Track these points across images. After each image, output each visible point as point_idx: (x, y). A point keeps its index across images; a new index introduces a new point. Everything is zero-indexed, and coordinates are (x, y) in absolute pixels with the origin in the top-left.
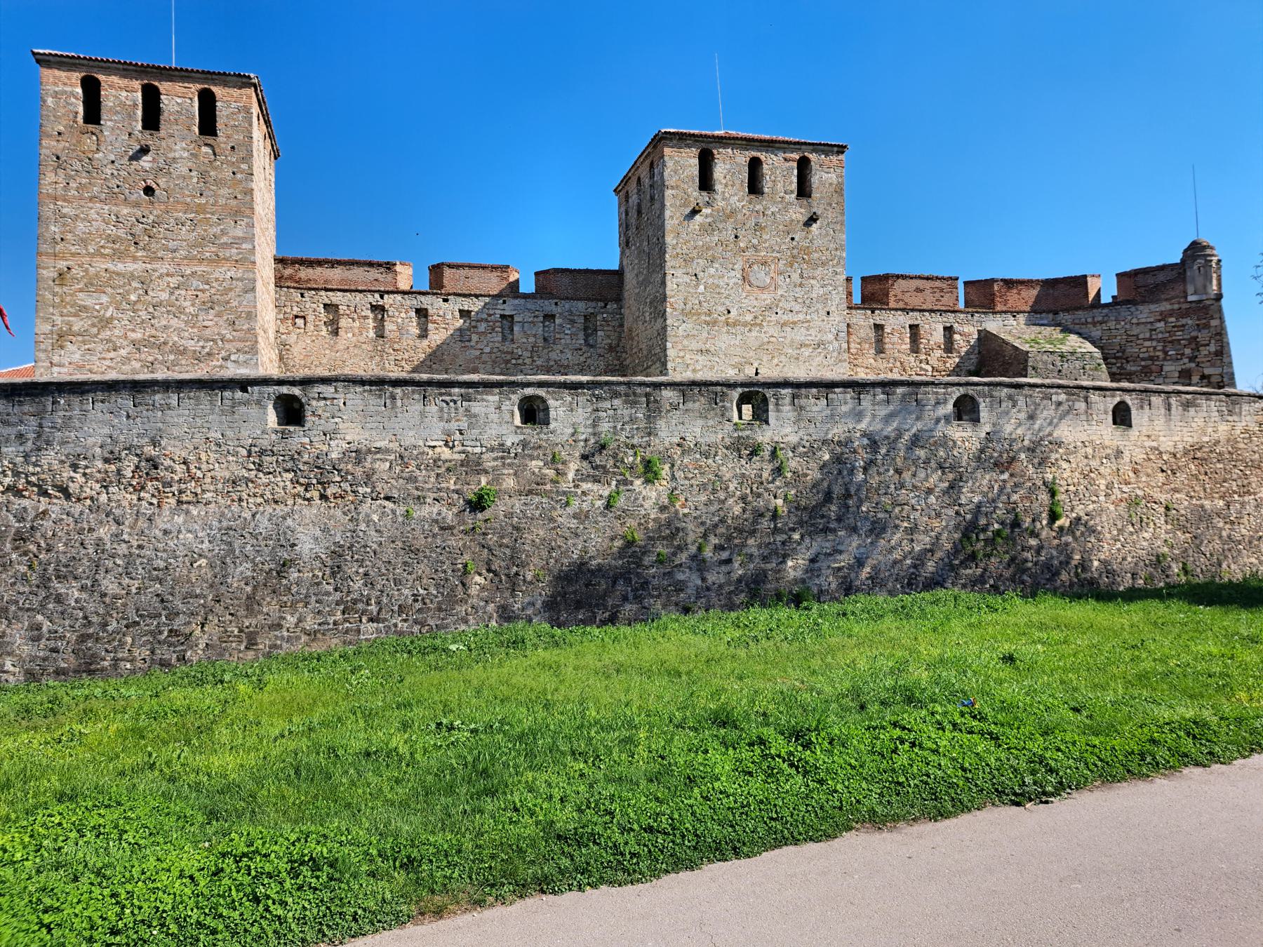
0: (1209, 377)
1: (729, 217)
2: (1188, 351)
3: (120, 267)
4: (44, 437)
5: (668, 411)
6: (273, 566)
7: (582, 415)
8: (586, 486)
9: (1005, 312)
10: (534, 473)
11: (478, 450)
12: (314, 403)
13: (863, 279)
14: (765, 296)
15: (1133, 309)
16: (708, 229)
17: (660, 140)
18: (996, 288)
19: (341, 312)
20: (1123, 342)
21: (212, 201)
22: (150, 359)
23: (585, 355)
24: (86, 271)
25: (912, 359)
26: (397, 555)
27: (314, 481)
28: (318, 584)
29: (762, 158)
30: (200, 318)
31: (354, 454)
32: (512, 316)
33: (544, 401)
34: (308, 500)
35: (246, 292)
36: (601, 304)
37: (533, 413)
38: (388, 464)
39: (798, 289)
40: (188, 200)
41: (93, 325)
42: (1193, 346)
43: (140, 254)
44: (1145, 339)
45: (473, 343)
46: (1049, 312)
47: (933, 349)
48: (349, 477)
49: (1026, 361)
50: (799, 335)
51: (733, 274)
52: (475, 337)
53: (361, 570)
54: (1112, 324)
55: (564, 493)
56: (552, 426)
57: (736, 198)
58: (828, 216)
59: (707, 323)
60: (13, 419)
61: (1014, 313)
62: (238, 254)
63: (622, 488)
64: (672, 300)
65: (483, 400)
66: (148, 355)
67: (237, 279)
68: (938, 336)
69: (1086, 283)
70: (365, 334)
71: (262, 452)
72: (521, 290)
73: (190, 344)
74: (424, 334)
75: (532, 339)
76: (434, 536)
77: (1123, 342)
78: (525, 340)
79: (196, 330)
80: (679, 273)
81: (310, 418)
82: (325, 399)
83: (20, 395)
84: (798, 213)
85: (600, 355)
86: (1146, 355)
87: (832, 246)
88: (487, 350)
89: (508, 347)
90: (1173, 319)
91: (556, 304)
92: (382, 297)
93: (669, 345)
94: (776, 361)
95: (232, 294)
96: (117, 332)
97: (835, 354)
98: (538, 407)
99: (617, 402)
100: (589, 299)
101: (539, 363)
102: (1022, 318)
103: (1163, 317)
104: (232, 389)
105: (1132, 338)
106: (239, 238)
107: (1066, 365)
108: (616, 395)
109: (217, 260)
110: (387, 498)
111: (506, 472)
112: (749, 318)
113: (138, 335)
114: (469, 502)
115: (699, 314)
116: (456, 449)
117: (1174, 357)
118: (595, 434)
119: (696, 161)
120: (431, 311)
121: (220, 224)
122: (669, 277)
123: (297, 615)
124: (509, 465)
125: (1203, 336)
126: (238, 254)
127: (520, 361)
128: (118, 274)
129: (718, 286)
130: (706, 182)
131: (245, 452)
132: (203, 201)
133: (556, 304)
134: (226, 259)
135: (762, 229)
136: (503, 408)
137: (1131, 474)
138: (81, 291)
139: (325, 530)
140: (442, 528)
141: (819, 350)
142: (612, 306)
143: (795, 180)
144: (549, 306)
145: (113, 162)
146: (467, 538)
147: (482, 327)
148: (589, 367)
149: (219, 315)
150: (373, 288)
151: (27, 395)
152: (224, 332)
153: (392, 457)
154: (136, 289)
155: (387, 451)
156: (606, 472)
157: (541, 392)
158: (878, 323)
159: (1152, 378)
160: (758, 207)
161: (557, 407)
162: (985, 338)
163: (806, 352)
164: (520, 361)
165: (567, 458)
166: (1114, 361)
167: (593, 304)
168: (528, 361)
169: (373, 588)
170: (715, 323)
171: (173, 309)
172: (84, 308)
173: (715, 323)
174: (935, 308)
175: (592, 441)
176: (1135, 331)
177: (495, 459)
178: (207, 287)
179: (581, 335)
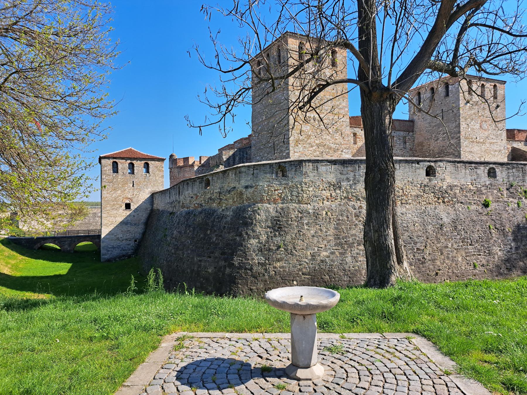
4: (356, 179)
6: (439, 226)
9: (518, 141)
11: (479, 186)
12: (438, 168)
14: (486, 133)
18: (515, 132)
22: (322, 151)
30: (335, 136)
34: (439, 203)
36: (408, 133)
39: (494, 131)
41: (306, 138)
50: (495, 147)
51: (478, 125)
55: (506, 202)
56: (497, 178)
59: (471, 142)
60: (344, 172)
61: (520, 141)
63: (520, 200)
65: (480, 169)
66: (321, 149)
71: (425, 186)
73: (333, 146)
74: (355, 143)
80: (464, 123)
81: (437, 174)
82: (441, 167)
83: (346, 164)
87: (503, 116)
94: (489, 156)
95: (343, 127)
99: (514, 170)
100: (404, 131)
102: (523, 143)
104: (415, 163)
106: (344, 106)
108: (513, 168)
110: (461, 203)
112: (482, 140)
113: (317, 142)
114: (484, 204)
115: (469, 139)
120: (358, 134)
122: (461, 125)
123: (451, 243)
124: (489, 192)
129: (474, 129)
131: (419, 186)
136: (485, 171)
139: (448, 213)
140: (479, 213)
142: (411, 134)
146: (487, 217)
151: (349, 164)
153: (459, 188)
156: (515, 195)
157: (494, 166)
163: (497, 153)
165: (503, 189)
167: (405, 133)
169: (467, 234)
175: (508, 184)
179: (402, 144)
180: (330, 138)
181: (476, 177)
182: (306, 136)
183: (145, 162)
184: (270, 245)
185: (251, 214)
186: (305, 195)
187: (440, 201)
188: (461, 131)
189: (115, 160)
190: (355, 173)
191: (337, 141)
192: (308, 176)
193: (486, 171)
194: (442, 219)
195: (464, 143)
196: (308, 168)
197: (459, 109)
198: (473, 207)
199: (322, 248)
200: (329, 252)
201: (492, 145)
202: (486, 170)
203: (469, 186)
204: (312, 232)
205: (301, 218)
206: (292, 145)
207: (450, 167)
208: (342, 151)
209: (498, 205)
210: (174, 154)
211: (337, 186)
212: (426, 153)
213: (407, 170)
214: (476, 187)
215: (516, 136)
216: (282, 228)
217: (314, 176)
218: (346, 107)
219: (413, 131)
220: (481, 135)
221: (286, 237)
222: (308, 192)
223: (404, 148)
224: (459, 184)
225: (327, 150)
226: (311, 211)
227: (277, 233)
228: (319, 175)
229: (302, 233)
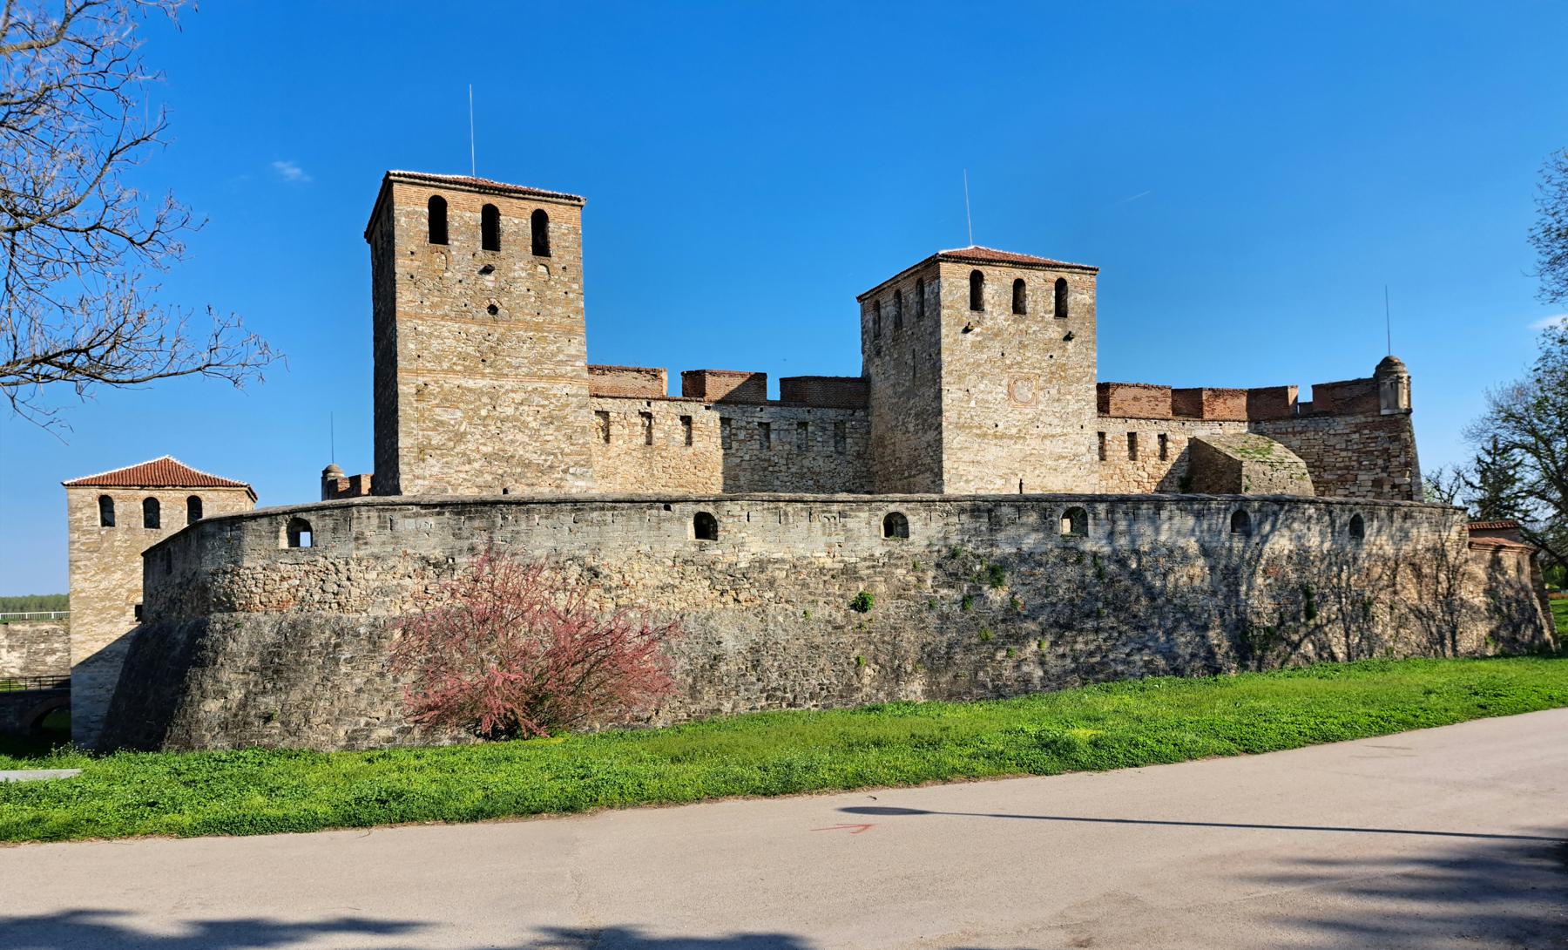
0: (1399, 486)
1: (996, 335)
2: (1380, 462)
3: (470, 383)
5: (1007, 525)
7: (935, 527)
9: (1213, 420)
10: (899, 580)
14: (1027, 411)
15: (1330, 421)
16: (978, 347)
17: (932, 263)
18: (1204, 398)
19: (611, 419)
20: (1321, 452)
21: (548, 319)
22: (500, 472)
23: (835, 462)
24: (441, 387)
25: (1130, 467)
26: (802, 652)
27: (728, 588)
28: (744, 675)
29: (1025, 279)
30: (542, 433)
31: (757, 564)
33: (903, 517)
35: (581, 408)
36: (849, 412)
37: (895, 526)
39: (1056, 404)
40: (528, 318)
42: (1385, 457)
43: (487, 371)
44: (1341, 450)
45: (733, 451)
47: (1148, 457)
48: (757, 584)
49: (1240, 470)
50: (1057, 447)
51: (1000, 389)
52: (735, 445)
53: (776, 664)
54: (1311, 435)
56: (912, 537)
57: (1003, 317)
58: (1082, 335)
59: (978, 435)
62: (573, 371)
64: (947, 414)
65: (856, 516)
67: (573, 396)
68: (1154, 444)
69: (1287, 394)
70: (635, 441)
72: (769, 398)
74: (689, 442)
75: (787, 447)
76: (830, 634)
77: (1321, 452)
78: (781, 448)
79: (538, 444)
80: (953, 388)
81: (721, 534)
82: (733, 516)
84: (1055, 332)
85: (849, 463)
86: (1342, 465)
88: (747, 457)
89: (765, 454)
90: (1367, 431)
91: (809, 412)
92: (649, 404)
93: (945, 457)
94: (1037, 472)
95: (568, 410)
96: (470, 446)
97: (1088, 466)
98: (896, 522)
100: (839, 407)
101: (793, 470)
103: (1358, 429)
105: (1328, 449)
106: (573, 356)
107: (1275, 475)
109: (555, 377)
110: (787, 602)
111: (878, 579)
112: (1014, 431)
113: (487, 449)
115: (971, 427)
116: (835, 559)
117: (1368, 467)
118: (946, 546)
120: (695, 419)
121: (555, 343)
124: (880, 573)
125: (1394, 448)
126: (573, 371)
127: (776, 469)
128: (470, 390)
130: (976, 303)
132: (540, 319)
134: (563, 376)
135: (1025, 346)
138: (438, 406)
139: (743, 629)
141: (1075, 462)
142: (859, 414)
143: (1054, 301)
144: (801, 413)
145: (460, 281)
147: (742, 435)
149: (558, 429)
150: (641, 396)
152: (563, 446)
154: (485, 405)
155: (783, 561)
159: (1347, 486)
160: (1022, 326)
161: (915, 523)
162: (1195, 444)
163: (1063, 463)
164: (776, 469)
165: (925, 567)
167: (842, 412)
168: (783, 468)
170: (985, 435)
171: (519, 424)
172: (442, 423)
173: (985, 435)
174: (1151, 416)
176: (1333, 441)
177: (868, 568)
178: (546, 403)
179: (832, 442)
180: (527, 440)
181: (842, 538)
182: (451, 435)
183: (145, 494)
184: (248, 715)
185: (218, 640)
186: (355, 592)
187: (728, 598)
188: (944, 407)
189: (104, 492)
190: (491, 533)
191: (548, 446)
192: (366, 544)
193: (878, 522)
194: (719, 643)
195: (952, 439)
196: (365, 521)
197: (939, 353)
198: (821, 612)
199: (378, 719)
200: (395, 728)
201: (1047, 442)
202: (876, 518)
203: (822, 560)
204: (357, 680)
205: (337, 645)
206: (406, 460)
207: (760, 515)
208: (565, 471)
209: (897, 607)
210: (335, 466)
211: (442, 567)
212: (890, 464)
213: (636, 523)
214: (842, 561)
215: (1206, 408)
216: (282, 672)
217: (384, 543)
218: (577, 357)
219: (866, 407)
220: (1009, 419)
221: (288, 694)
222: (363, 582)
223: (837, 452)
224: (788, 556)
225: (519, 470)
226: (362, 630)
227: (269, 686)
228: (396, 539)
229: (330, 684)
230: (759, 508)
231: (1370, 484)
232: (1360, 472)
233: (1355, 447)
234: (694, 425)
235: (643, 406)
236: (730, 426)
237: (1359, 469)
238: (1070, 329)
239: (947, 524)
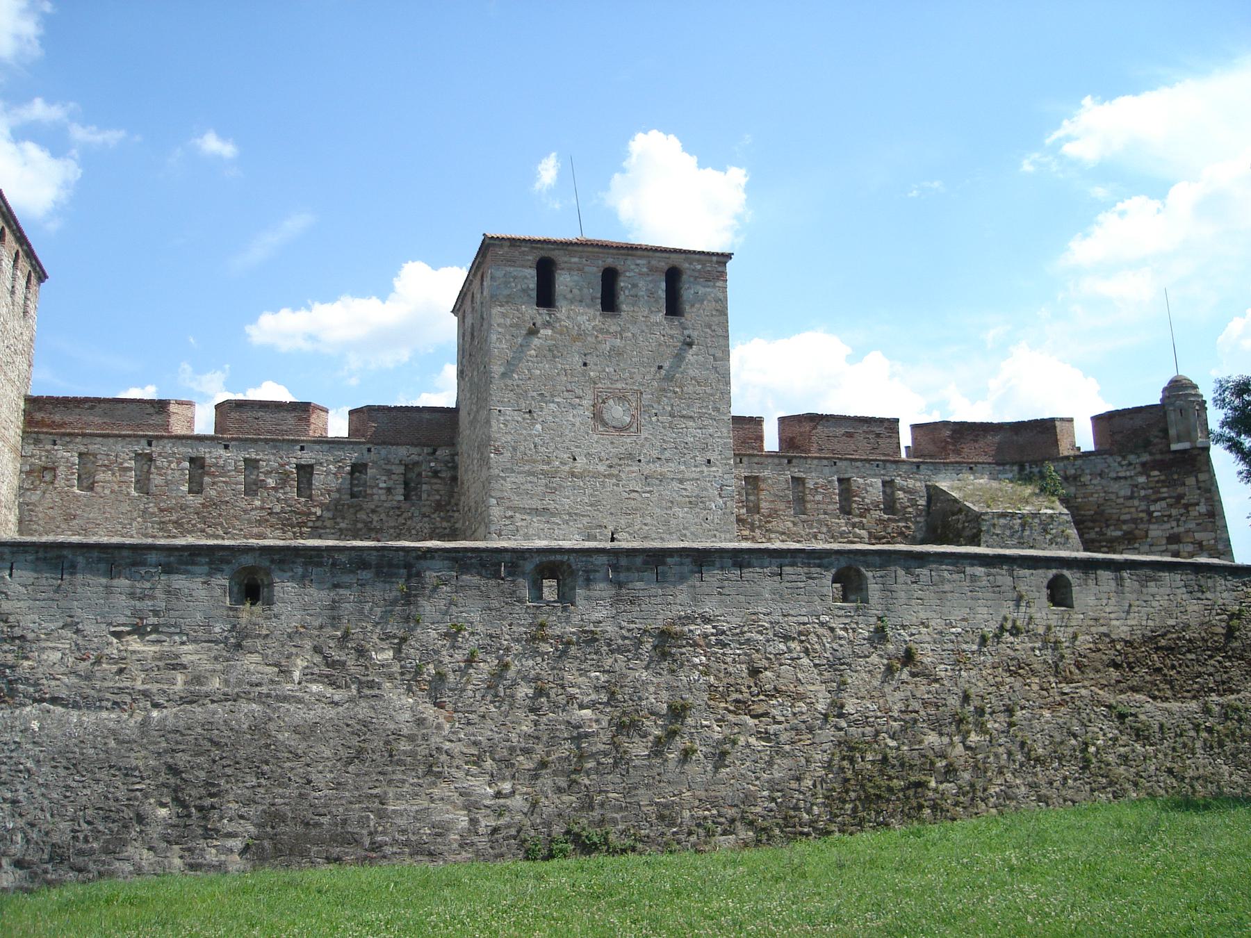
8: (315, 688)
13: (782, 420)
23: (405, 515)
32: (311, 466)
36: (426, 450)
38: (59, 655)
46: (1013, 464)
69: (1055, 427)
72: (331, 434)
85: (424, 515)
91: (369, 450)
92: (150, 444)
100: (413, 445)
101: (342, 525)
112: (602, 468)
115: (535, 462)
119: (533, 272)
120: (208, 461)
133: (369, 450)
137: (1073, 668)
143: (663, 295)
148: (409, 530)
158: (796, 475)
162: (934, 494)
166: (1090, 524)
230: (30, 557)
231: (1164, 542)
232: (1152, 527)
233: (1143, 493)
234: (207, 468)
235: (139, 448)
236: (258, 468)
237: (1149, 522)
238: (686, 332)
239: (336, 586)
